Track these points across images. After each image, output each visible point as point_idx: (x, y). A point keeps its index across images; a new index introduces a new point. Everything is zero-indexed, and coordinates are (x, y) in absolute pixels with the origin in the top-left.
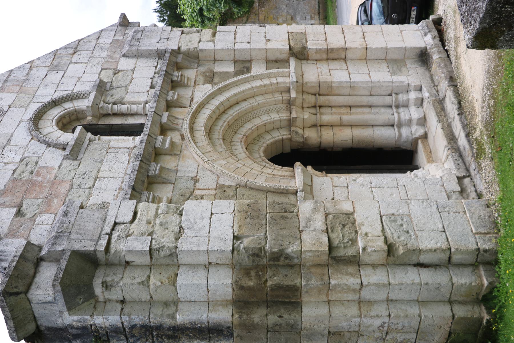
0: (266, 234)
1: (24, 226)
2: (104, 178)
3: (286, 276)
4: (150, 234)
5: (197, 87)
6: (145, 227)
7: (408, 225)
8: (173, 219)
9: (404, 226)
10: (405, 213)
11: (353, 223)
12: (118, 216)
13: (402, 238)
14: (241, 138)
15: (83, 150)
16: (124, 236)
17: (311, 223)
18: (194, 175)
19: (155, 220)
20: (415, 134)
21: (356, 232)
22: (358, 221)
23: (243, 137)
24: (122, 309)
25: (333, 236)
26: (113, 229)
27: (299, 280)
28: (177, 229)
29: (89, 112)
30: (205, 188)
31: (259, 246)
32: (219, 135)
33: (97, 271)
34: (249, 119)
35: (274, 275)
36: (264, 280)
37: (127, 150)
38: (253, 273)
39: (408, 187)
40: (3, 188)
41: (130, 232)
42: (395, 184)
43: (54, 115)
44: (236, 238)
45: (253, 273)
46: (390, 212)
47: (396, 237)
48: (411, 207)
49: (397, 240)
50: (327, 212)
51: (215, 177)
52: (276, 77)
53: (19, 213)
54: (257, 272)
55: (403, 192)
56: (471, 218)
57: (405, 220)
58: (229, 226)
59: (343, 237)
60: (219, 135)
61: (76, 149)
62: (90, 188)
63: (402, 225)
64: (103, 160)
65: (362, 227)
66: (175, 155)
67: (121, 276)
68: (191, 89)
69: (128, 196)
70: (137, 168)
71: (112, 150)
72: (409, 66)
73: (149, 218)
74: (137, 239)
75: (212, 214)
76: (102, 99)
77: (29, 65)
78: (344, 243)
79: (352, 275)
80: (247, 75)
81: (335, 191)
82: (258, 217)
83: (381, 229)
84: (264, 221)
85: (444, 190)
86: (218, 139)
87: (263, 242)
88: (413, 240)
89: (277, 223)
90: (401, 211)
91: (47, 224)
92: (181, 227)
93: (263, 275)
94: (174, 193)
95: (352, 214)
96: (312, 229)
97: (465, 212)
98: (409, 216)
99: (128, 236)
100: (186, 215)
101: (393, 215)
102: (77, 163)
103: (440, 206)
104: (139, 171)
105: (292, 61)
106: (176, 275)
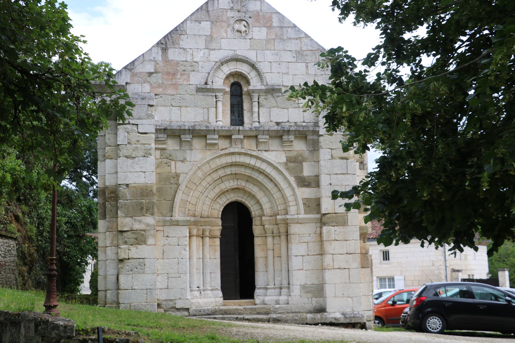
0: (130, 200)
1: (140, 79)
2: (180, 111)
3: (111, 211)
4: (129, 143)
5: (283, 152)
6: (133, 140)
7: (137, 271)
8: (140, 153)
9: (136, 270)
10: (145, 271)
11: (138, 244)
12: (142, 125)
13: (127, 267)
15: (206, 94)
16: (127, 131)
17: (138, 223)
18: (188, 159)
19: (140, 144)
20: (257, 298)
21: (132, 245)
22: (139, 246)
23: (243, 186)
24: (102, 136)
25: (129, 233)
26: (133, 124)
27: (108, 217)
28: (134, 156)
29: (251, 88)
30: (177, 167)
31: (121, 197)
32: (238, 171)
33: (113, 121)
35: (111, 205)
36: (109, 200)
37: (206, 119)
38: (112, 195)
39: (179, 279)
40: (170, 59)
41: (130, 133)
42: (182, 272)
43: (241, 68)
44: (127, 185)
45: (112, 195)
46: (146, 263)
47: (128, 264)
48: (151, 275)
49: (126, 265)
50: (146, 231)
51: (186, 171)
52: (297, 205)
53: (150, 74)
54: (113, 197)
55: (174, 275)
56: (142, 305)
57: (140, 270)
58: (135, 181)
59: (129, 238)
60: (238, 171)
61: (204, 90)
62: (172, 105)
63: (137, 268)
64: (197, 107)
65: (135, 248)
66: (206, 147)
67: (110, 133)
68: (280, 149)
69: (158, 127)
70: (182, 128)
71: (206, 110)
72: (314, 300)
73: (141, 141)
74: (125, 137)
75: (145, 172)
76: (260, 94)
77: (303, 35)
78: (124, 238)
79: (112, 242)
80: (294, 185)
81: (175, 238)
82: (142, 196)
83: (134, 258)
84: (139, 199)
85: (176, 298)
86: (231, 171)
87: (124, 199)
88: (125, 272)
89: (137, 206)
90: (147, 269)
91: (142, 90)
92: (135, 158)
93: (112, 200)
94: (172, 151)
95: (145, 244)
96: (133, 223)
97: (147, 302)
98: (144, 273)
99: (128, 133)
100: (143, 159)
101: (145, 265)
102: (195, 93)
103: (151, 290)
104: (180, 130)
105: (318, 216)
106: (112, 159)
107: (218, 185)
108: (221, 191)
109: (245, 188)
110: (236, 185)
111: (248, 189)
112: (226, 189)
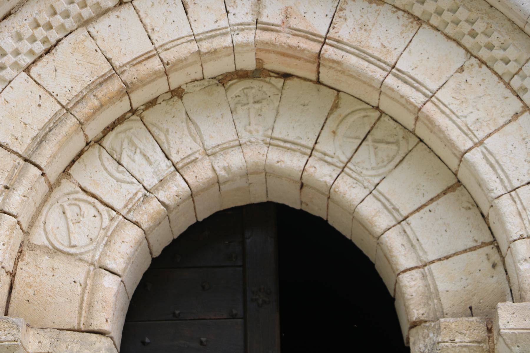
14: (294, 23)
23: (309, 36)
34: (484, 54)
107: (85, 23)
108: (105, 80)
109: (329, 52)
110: (242, 27)
111: (352, 60)
112: (155, 64)
